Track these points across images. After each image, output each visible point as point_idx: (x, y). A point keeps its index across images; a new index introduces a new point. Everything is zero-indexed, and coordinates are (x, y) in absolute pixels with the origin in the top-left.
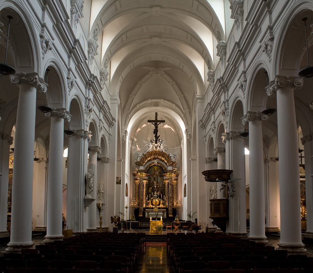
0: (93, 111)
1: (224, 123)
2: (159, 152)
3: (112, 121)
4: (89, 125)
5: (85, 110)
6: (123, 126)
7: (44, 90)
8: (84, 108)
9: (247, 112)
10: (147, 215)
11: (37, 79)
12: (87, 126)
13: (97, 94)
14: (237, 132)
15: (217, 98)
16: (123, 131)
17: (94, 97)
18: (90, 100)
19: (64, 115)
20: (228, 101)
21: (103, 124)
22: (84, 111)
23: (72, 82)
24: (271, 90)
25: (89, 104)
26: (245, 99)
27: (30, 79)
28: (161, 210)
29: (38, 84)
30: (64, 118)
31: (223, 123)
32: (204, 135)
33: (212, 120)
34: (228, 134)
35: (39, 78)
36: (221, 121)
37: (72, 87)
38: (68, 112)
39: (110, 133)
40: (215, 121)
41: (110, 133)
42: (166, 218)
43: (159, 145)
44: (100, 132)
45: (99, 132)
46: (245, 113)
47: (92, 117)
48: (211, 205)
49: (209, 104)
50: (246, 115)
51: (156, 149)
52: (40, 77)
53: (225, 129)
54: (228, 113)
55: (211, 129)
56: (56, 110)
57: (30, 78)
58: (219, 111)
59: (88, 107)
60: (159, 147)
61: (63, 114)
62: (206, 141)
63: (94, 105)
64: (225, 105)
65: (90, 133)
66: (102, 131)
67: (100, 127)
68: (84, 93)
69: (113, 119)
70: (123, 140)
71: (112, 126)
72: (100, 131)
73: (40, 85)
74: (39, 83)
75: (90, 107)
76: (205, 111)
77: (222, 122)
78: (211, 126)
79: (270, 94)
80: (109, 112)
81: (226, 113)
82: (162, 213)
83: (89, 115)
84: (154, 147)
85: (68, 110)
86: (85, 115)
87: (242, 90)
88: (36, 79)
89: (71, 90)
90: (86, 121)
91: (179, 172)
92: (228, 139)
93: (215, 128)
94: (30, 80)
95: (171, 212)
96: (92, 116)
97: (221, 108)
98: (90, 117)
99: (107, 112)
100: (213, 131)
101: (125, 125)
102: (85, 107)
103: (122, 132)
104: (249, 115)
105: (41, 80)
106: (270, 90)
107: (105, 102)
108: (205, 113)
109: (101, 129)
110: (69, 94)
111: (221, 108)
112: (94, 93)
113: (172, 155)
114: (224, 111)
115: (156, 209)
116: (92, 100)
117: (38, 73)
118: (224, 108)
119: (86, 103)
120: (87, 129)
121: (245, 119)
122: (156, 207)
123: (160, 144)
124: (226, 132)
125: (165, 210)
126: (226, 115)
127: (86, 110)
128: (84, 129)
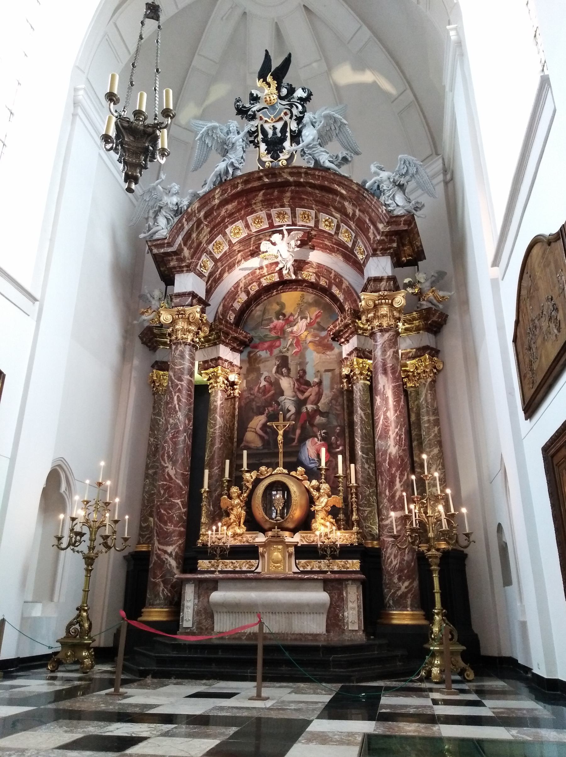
2: (297, 171)
10: (197, 613)
28: (315, 565)
42: (361, 637)
43: (293, 126)
51: (275, 157)
60: (296, 137)
82: (322, 596)
84: (263, 146)
91: (441, 294)
95: (404, 586)
113: (384, 175)
115: (277, 555)
122: (282, 542)
125: (354, 565)
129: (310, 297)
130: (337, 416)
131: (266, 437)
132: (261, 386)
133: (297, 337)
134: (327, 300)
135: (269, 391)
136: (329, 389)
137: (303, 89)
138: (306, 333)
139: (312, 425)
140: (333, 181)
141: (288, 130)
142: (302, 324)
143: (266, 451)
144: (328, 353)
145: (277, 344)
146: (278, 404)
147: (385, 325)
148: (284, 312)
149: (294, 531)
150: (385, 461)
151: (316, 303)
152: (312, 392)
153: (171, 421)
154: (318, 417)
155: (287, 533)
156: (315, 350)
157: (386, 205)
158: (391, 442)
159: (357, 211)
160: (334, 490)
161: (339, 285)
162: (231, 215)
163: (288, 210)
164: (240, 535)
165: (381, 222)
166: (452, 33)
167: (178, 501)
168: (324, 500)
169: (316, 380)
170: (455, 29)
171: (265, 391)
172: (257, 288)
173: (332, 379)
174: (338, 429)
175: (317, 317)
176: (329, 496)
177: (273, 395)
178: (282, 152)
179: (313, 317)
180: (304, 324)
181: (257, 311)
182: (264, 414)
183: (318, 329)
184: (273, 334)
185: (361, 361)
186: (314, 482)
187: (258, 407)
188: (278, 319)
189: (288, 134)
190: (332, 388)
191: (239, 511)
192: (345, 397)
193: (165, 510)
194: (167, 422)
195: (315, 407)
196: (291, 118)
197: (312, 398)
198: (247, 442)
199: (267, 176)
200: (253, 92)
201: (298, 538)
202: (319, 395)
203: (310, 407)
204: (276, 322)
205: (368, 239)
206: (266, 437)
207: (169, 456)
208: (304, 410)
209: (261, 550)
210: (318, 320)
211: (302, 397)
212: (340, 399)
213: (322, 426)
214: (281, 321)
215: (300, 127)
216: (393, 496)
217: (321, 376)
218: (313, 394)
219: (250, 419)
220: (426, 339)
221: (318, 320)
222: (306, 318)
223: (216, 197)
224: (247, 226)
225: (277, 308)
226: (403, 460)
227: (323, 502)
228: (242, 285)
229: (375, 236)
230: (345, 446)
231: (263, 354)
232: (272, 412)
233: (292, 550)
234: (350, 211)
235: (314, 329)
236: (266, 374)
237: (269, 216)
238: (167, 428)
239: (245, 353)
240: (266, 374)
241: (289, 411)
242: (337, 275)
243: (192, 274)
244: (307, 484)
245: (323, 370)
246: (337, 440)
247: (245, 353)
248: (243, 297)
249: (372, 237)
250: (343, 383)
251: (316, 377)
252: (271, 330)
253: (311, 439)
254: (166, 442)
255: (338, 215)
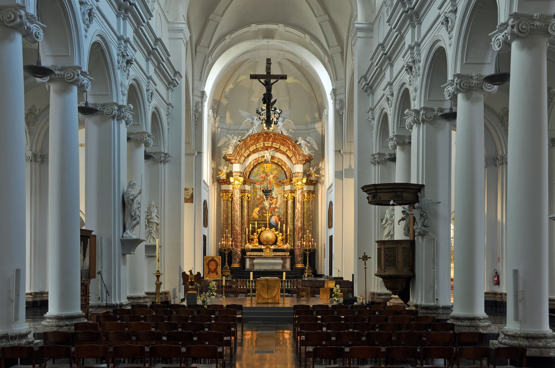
0: (134, 63)
1: (411, 89)
2: (275, 134)
3: (174, 76)
4: (126, 92)
5: (119, 63)
6: (196, 82)
7: (38, 38)
8: (116, 58)
9: (455, 76)
11: (24, 18)
12: (123, 95)
13: (143, 26)
14: (436, 108)
15: (397, 35)
16: (196, 93)
17: (136, 32)
18: (127, 41)
19: (77, 80)
20: (418, 45)
21: (155, 85)
22: (117, 64)
23: (91, 10)
24: (501, 40)
25: (126, 50)
26: (452, 47)
27: (9, 18)
29: (26, 27)
30: (77, 86)
31: (408, 88)
32: (371, 106)
33: (387, 79)
34: (417, 112)
35: (27, 14)
36: (404, 83)
37: (91, 21)
38: (85, 73)
39: (170, 101)
40: (392, 81)
41: (170, 101)
44: (150, 103)
45: (147, 103)
46: (450, 77)
47: (132, 73)
48: (379, 249)
49: (382, 45)
50: (451, 80)
51: (268, 129)
52: (28, 11)
53: (412, 102)
54: (419, 70)
55: (385, 97)
56: (60, 70)
57: (9, 16)
58: (400, 63)
59: (123, 56)
61: (76, 77)
62: (373, 119)
63: (135, 51)
64: (412, 54)
65: (130, 108)
66: (153, 99)
67: (150, 91)
68: (115, 28)
69: (176, 73)
70: (196, 111)
71: (175, 86)
72: (150, 100)
73: (29, 28)
74: (28, 24)
75: (128, 55)
76: (371, 59)
77: (407, 86)
78: (384, 90)
79: (499, 46)
80: (168, 60)
81: (414, 70)
83: (127, 72)
85: (85, 69)
86: (119, 72)
87: (447, 29)
88: (21, 17)
89: (88, 27)
90: (122, 85)
92: (417, 123)
93: (392, 95)
94: (8, 20)
96: (134, 71)
97: (403, 57)
98: (128, 75)
99: (163, 61)
100: (388, 100)
101: (200, 80)
102: (118, 55)
103: (194, 94)
104: (458, 82)
105: (30, 18)
106: (498, 39)
107: (158, 40)
108: (372, 64)
109: (151, 96)
110: (86, 37)
111: (403, 57)
112: (136, 25)
114: (411, 64)
116: (132, 40)
117: (22, 5)
118: (410, 60)
119: (119, 48)
120: (123, 100)
121: (451, 89)
122: (270, 248)
123: (277, 119)
124: (412, 108)
126: (413, 74)
127: (121, 62)
128: (118, 100)
129: (274, 166)
130: (282, 209)
131: (259, 215)
132: (258, 197)
133: (270, 181)
134: (280, 168)
135: (260, 200)
136: (280, 200)
137: (280, 110)
138: (273, 180)
139: (274, 211)
140: (286, 139)
141: (273, 121)
142: (271, 176)
143: (260, 219)
144: (280, 187)
145: (263, 183)
146: (264, 204)
147: (300, 188)
148: (265, 171)
149: (272, 245)
150: (297, 228)
151: (276, 169)
152: (274, 201)
153: (236, 214)
154: (276, 209)
155: (269, 246)
156: (275, 186)
157: (302, 151)
158: (299, 223)
159: (293, 149)
160: (283, 235)
161: (285, 166)
162: (251, 144)
163: (271, 143)
164: (257, 246)
165: (301, 156)
166: (326, 112)
167: (240, 237)
168: (280, 237)
169: (276, 197)
170: (327, 111)
171: (259, 199)
172: (257, 163)
173: (281, 196)
174: (282, 213)
175: (276, 174)
176: (282, 236)
177: (262, 201)
178: (270, 127)
179: (275, 174)
180: (272, 176)
181: (256, 170)
182: (258, 207)
183: (277, 179)
184: (261, 179)
185: (291, 194)
186: (277, 232)
187: (257, 205)
188: (263, 174)
189: (273, 122)
190: (281, 200)
191: (256, 240)
192: (285, 203)
193: (237, 239)
194: (235, 214)
195: (275, 206)
196: (275, 117)
197: (274, 203)
198: (253, 216)
199: (265, 134)
200: (263, 107)
201: (273, 247)
202: (277, 202)
203: (274, 206)
204: (262, 175)
205: (297, 159)
206: (259, 215)
207: (236, 224)
208: (272, 206)
209: (264, 250)
210: (277, 175)
211: (271, 202)
212: (283, 204)
213: (278, 212)
214: (264, 175)
215: (277, 120)
216: (299, 237)
217: (277, 195)
218: (275, 201)
219: (254, 209)
220: (312, 188)
221: (277, 175)
222: (273, 174)
223: (248, 140)
224: (256, 146)
225: (263, 169)
226: (302, 228)
227: (280, 238)
228: (252, 163)
229: (299, 158)
230: (284, 219)
231: (258, 186)
232: (261, 207)
233: (272, 250)
234: (291, 148)
235: (275, 178)
236: (259, 194)
237: (264, 144)
238: (235, 216)
239: (252, 186)
240: (259, 194)
241: (267, 207)
242: (284, 162)
243: (239, 164)
244: (275, 233)
245: (278, 193)
246: (282, 217)
247: (252, 186)
248: (252, 167)
249: (297, 158)
250: (284, 198)
251: (276, 196)
252: (261, 178)
253: (274, 216)
254: (235, 220)
255: (287, 148)
